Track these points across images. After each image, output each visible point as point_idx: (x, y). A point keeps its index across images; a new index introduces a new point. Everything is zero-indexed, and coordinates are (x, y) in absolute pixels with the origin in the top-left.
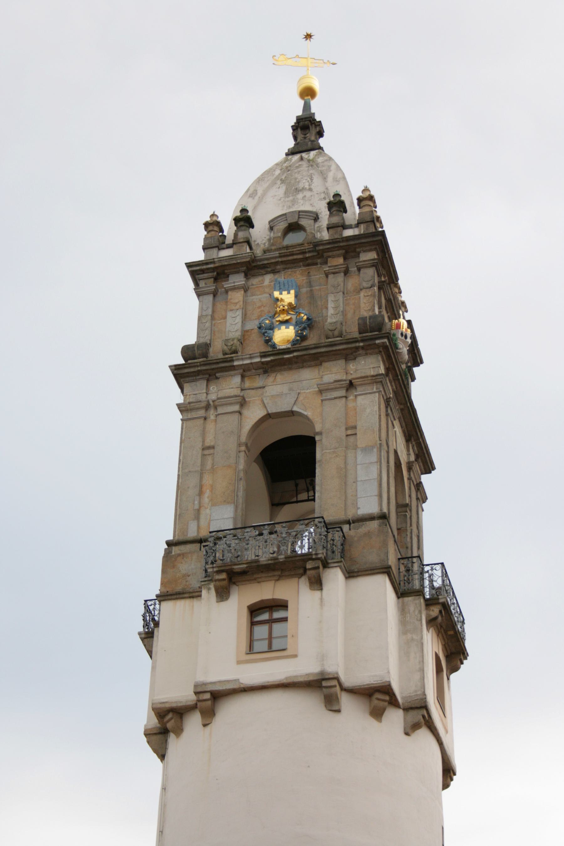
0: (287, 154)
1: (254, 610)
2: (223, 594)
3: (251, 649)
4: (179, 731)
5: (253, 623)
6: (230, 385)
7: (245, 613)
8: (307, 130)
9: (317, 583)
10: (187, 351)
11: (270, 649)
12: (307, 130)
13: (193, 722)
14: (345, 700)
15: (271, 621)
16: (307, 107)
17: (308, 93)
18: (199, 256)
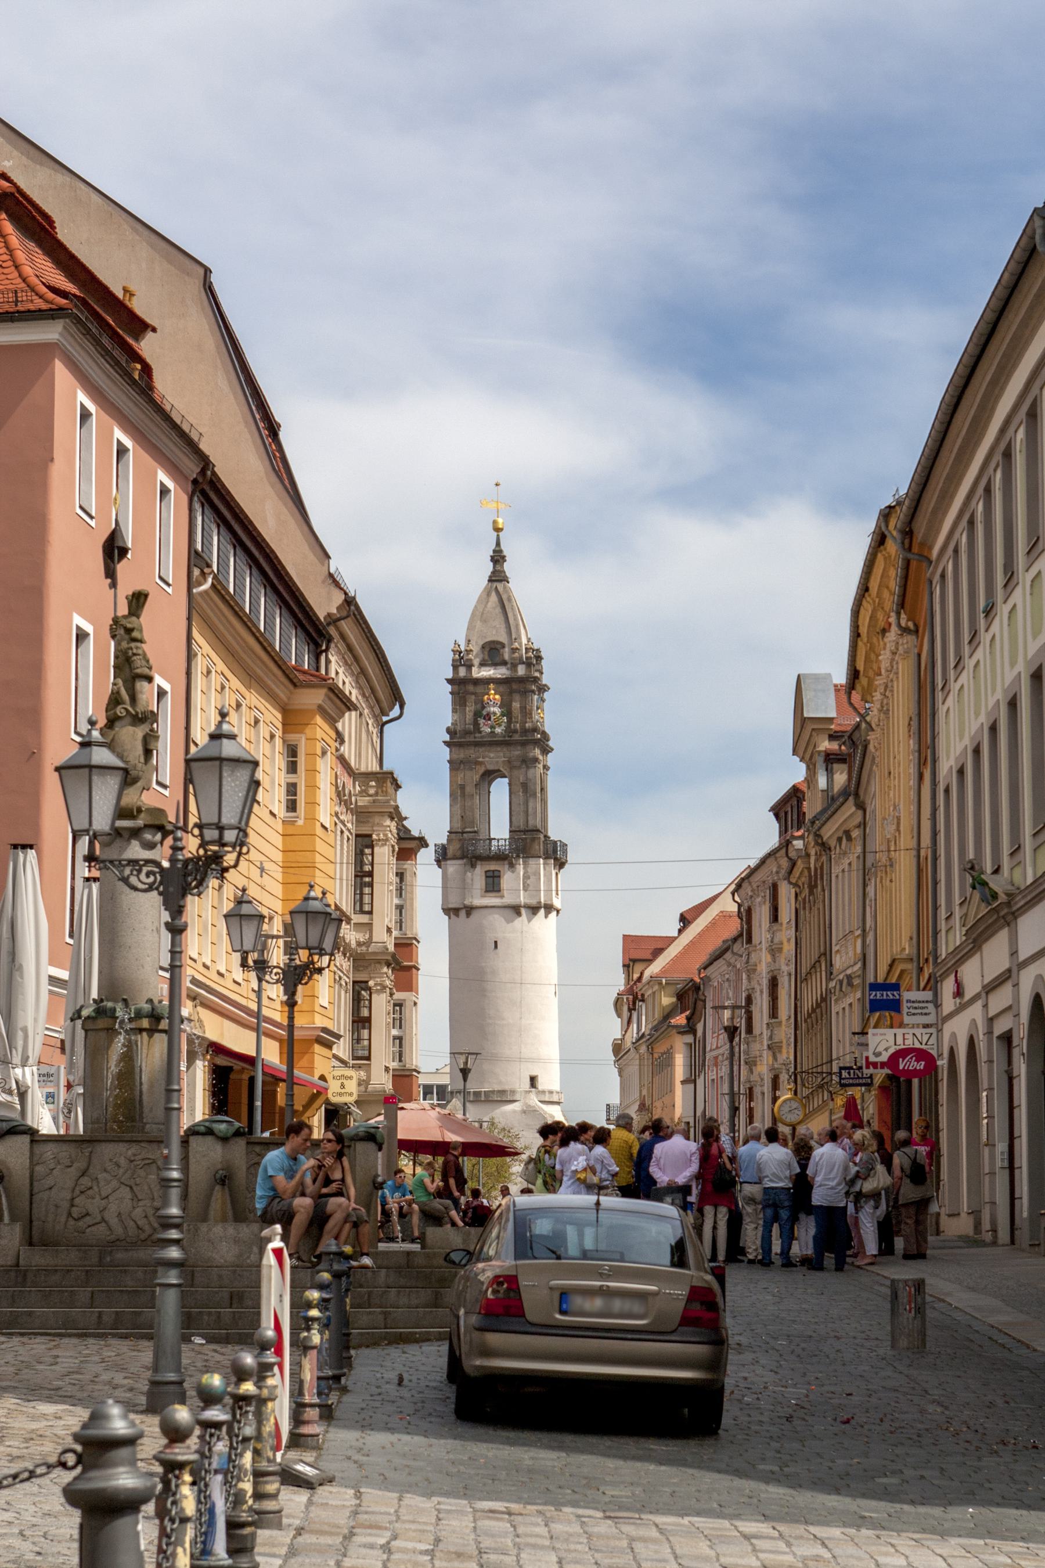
0: (490, 581)
1: (486, 872)
2: (473, 866)
3: (487, 891)
4: (457, 915)
5: (487, 877)
6: (471, 753)
7: (483, 874)
8: (498, 558)
9: (512, 866)
10: (448, 730)
11: (493, 891)
12: (498, 558)
13: (463, 913)
14: (523, 911)
15: (493, 877)
16: (498, 544)
17: (498, 530)
18: (450, 675)
